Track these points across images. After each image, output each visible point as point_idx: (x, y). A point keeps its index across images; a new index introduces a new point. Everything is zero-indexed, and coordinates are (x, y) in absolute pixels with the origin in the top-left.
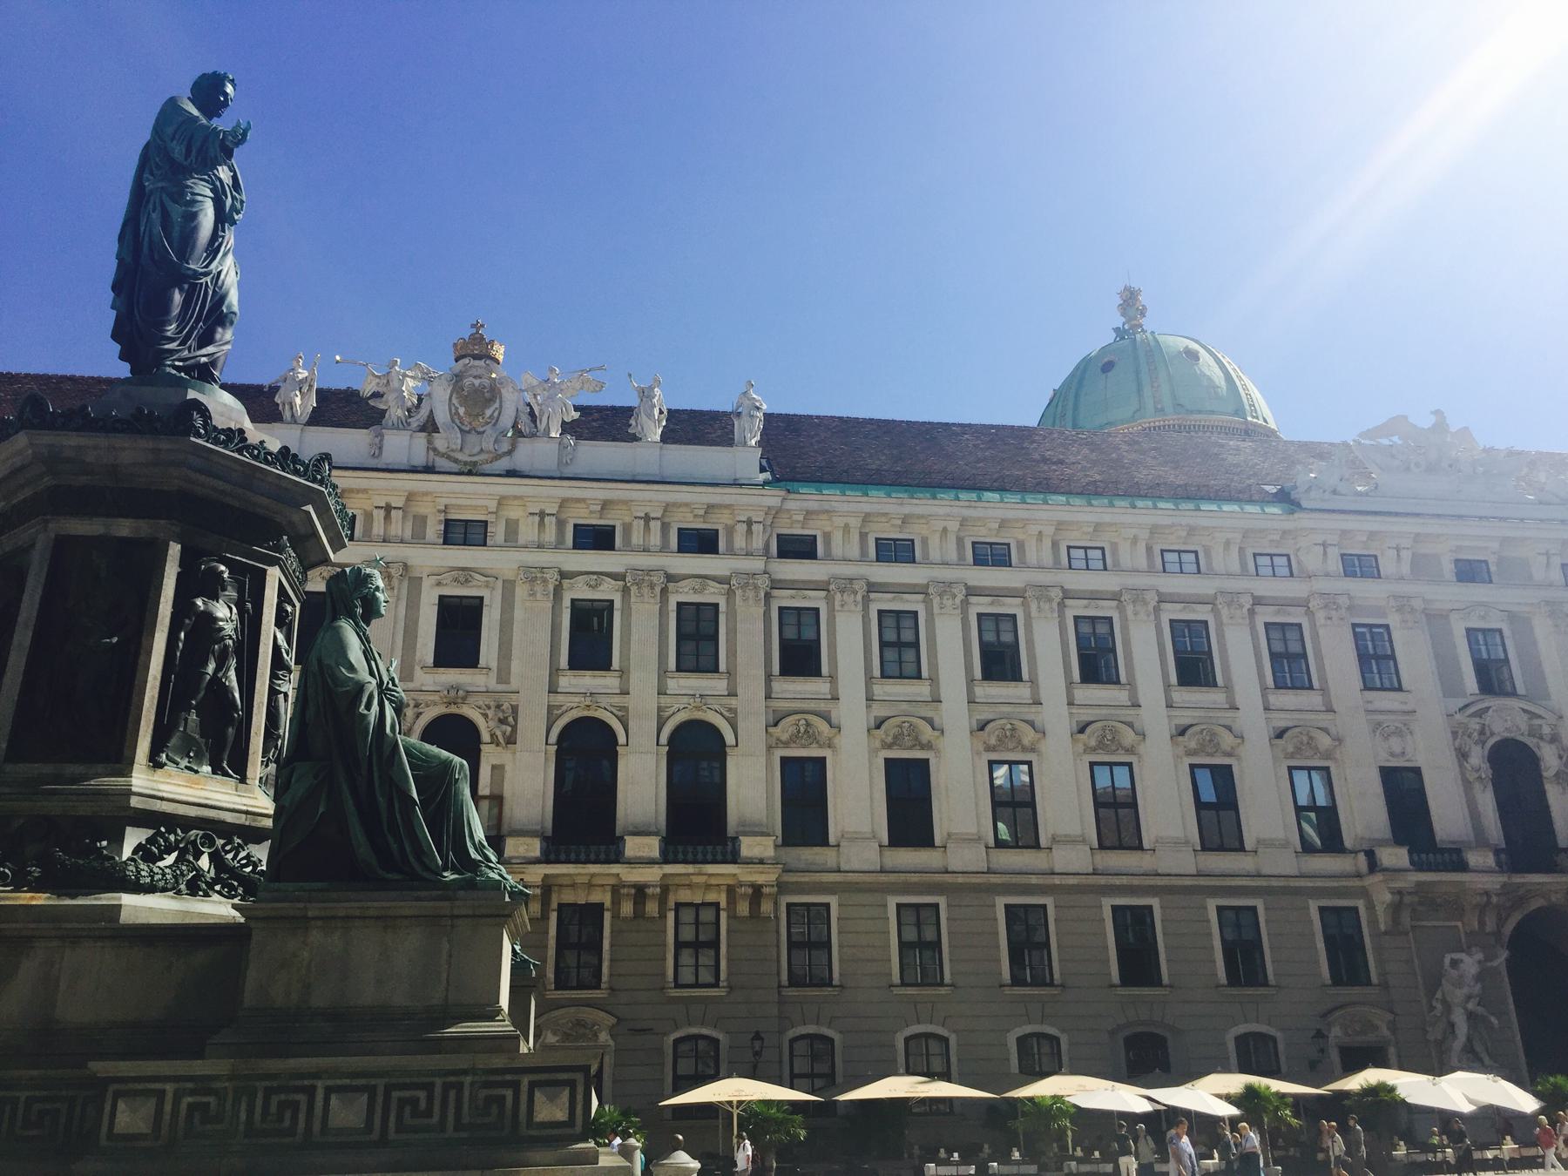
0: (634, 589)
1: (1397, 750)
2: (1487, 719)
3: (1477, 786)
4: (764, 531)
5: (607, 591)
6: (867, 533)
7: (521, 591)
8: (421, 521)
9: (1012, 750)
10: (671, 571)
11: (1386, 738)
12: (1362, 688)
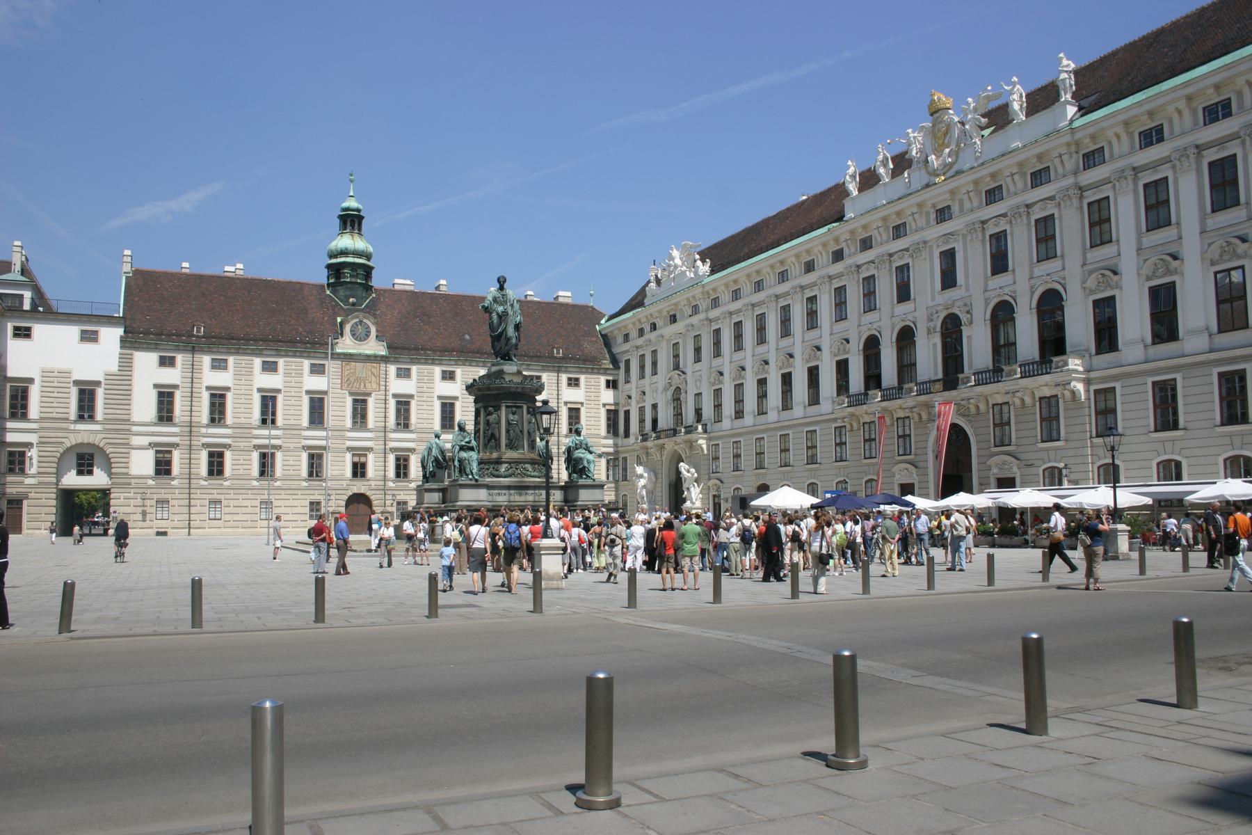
0: (1013, 219)
4: (1071, 157)
5: (1003, 225)
6: (1133, 131)
7: (969, 238)
8: (928, 214)
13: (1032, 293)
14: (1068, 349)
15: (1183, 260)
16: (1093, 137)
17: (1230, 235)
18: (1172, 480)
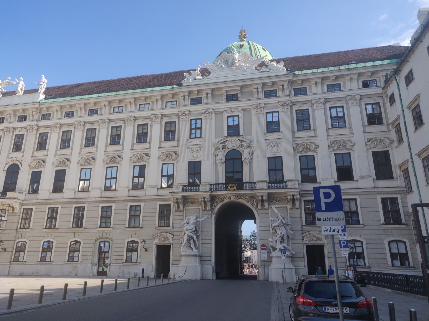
1: (195, 156)
2: (226, 143)
3: (219, 165)
4: (37, 114)
9: (87, 165)
10: (14, 127)
11: (193, 152)
12: (189, 138)
13: (6, 164)
14: (16, 190)
15: (71, 162)
16: (48, 109)
17: (89, 156)
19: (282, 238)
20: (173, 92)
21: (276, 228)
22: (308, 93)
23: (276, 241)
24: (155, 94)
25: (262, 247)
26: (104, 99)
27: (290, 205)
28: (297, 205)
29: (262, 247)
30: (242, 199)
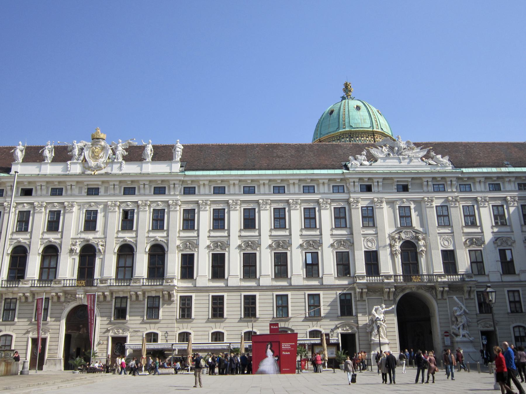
18: (184, 342)
19: (463, 325)
20: (342, 177)
21: (458, 317)
22: (473, 190)
23: (459, 329)
24: (323, 177)
25: (445, 334)
26: (264, 178)
27: (467, 296)
28: (472, 296)
29: (445, 334)
30: (422, 289)
